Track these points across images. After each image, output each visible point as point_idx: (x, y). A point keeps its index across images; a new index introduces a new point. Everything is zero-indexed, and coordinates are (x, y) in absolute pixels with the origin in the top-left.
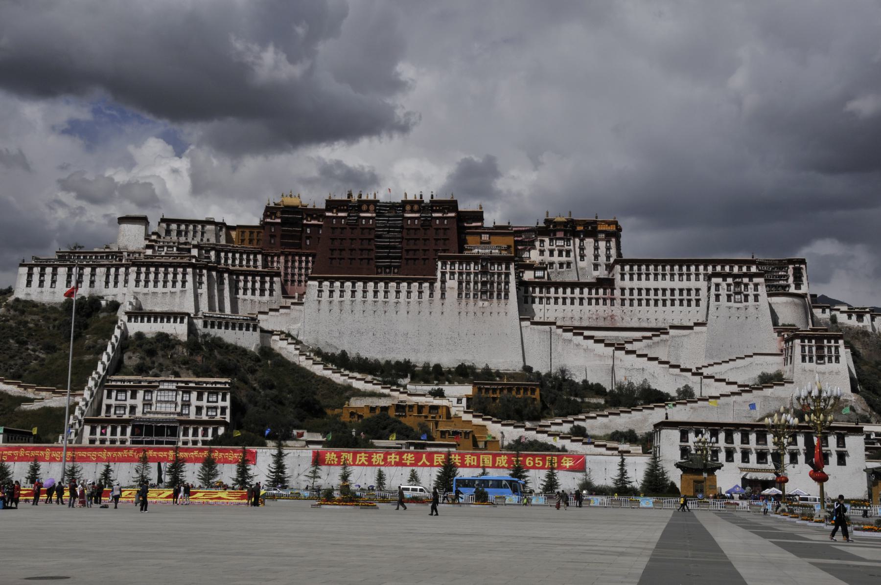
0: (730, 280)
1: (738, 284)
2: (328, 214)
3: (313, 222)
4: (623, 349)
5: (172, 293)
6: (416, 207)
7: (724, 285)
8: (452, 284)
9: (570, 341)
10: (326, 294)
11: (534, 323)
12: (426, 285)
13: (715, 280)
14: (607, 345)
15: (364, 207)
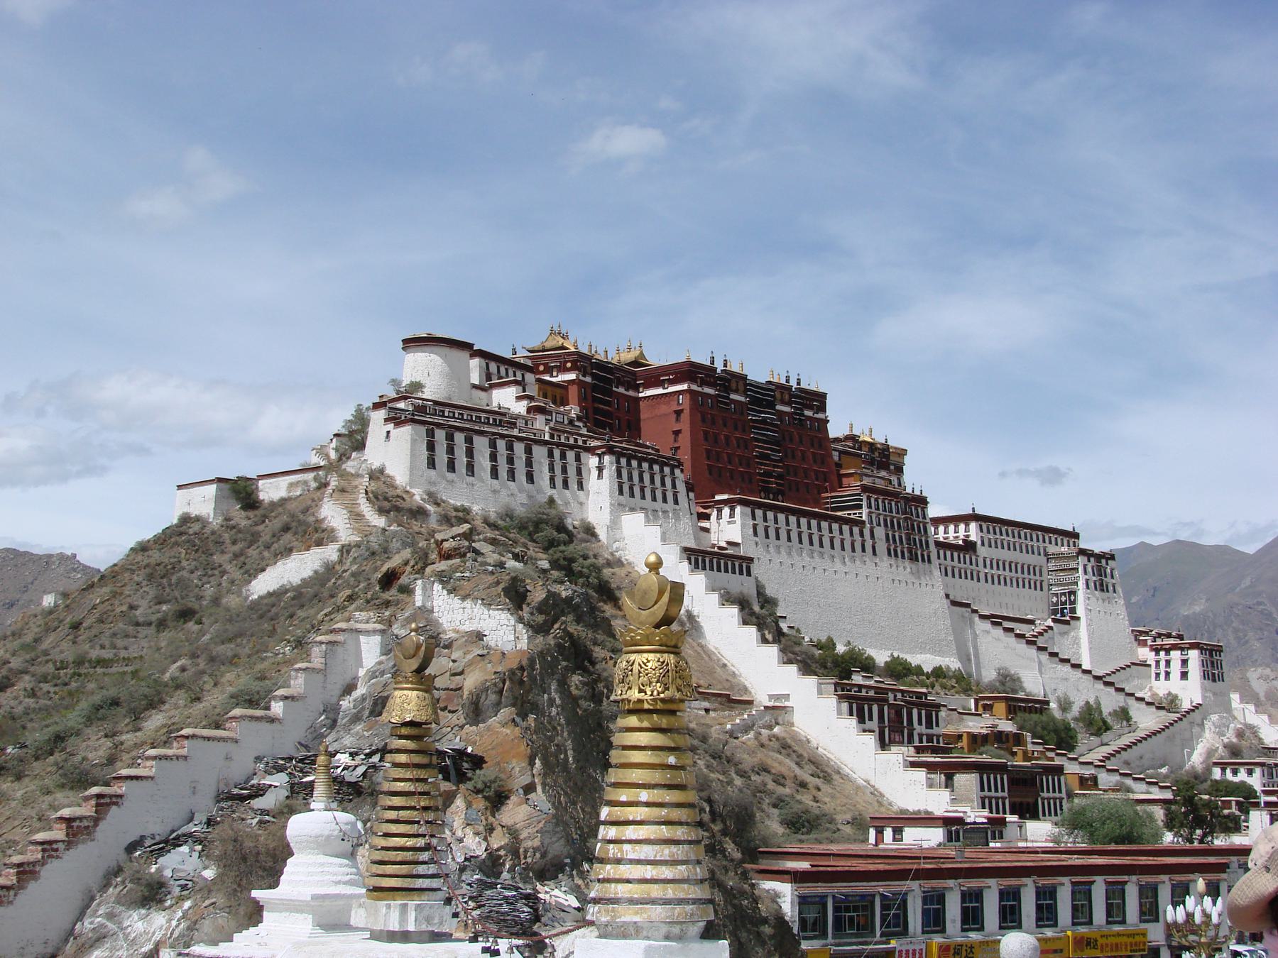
0: (1092, 559)
1: (1099, 568)
2: (694, 387)
3: (621, 390)
4: (1044, 649)
5: (665, 512)
6: (787, 397)
7: (1089, 569)
8: (880, 532)
9: (988, 632)
10: (761, 531)
11: (955, 603)
12: (856, 530)
13: (1082, 560)
14: (1029, 643)
15: (734, 386)
